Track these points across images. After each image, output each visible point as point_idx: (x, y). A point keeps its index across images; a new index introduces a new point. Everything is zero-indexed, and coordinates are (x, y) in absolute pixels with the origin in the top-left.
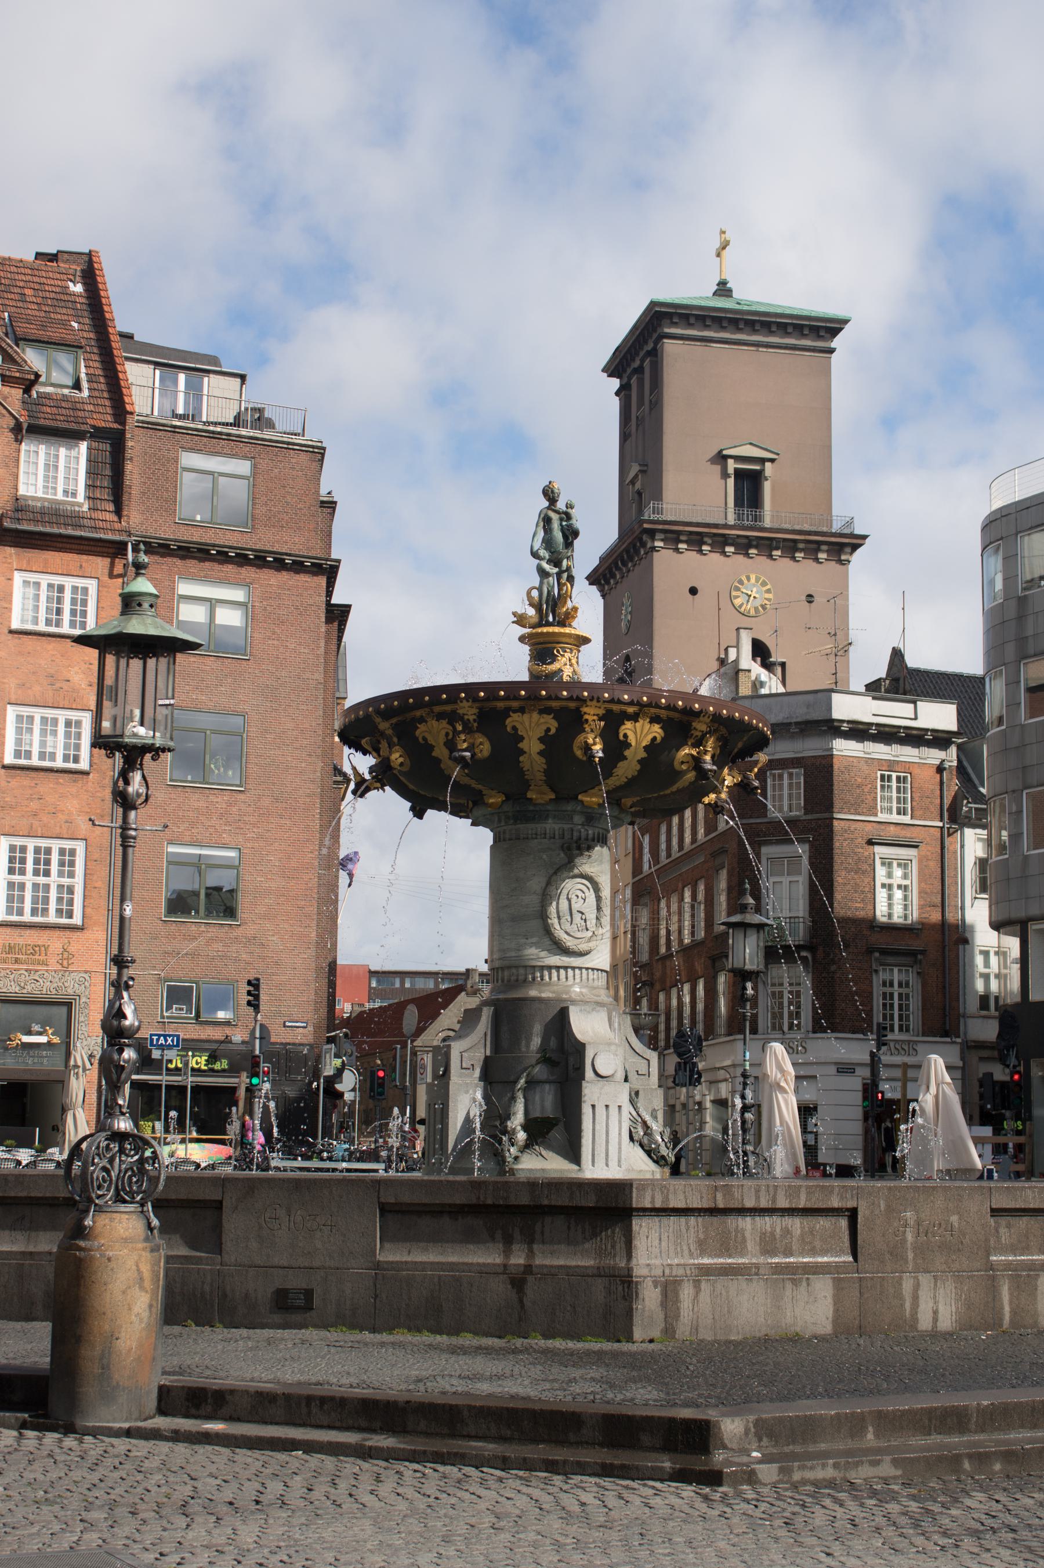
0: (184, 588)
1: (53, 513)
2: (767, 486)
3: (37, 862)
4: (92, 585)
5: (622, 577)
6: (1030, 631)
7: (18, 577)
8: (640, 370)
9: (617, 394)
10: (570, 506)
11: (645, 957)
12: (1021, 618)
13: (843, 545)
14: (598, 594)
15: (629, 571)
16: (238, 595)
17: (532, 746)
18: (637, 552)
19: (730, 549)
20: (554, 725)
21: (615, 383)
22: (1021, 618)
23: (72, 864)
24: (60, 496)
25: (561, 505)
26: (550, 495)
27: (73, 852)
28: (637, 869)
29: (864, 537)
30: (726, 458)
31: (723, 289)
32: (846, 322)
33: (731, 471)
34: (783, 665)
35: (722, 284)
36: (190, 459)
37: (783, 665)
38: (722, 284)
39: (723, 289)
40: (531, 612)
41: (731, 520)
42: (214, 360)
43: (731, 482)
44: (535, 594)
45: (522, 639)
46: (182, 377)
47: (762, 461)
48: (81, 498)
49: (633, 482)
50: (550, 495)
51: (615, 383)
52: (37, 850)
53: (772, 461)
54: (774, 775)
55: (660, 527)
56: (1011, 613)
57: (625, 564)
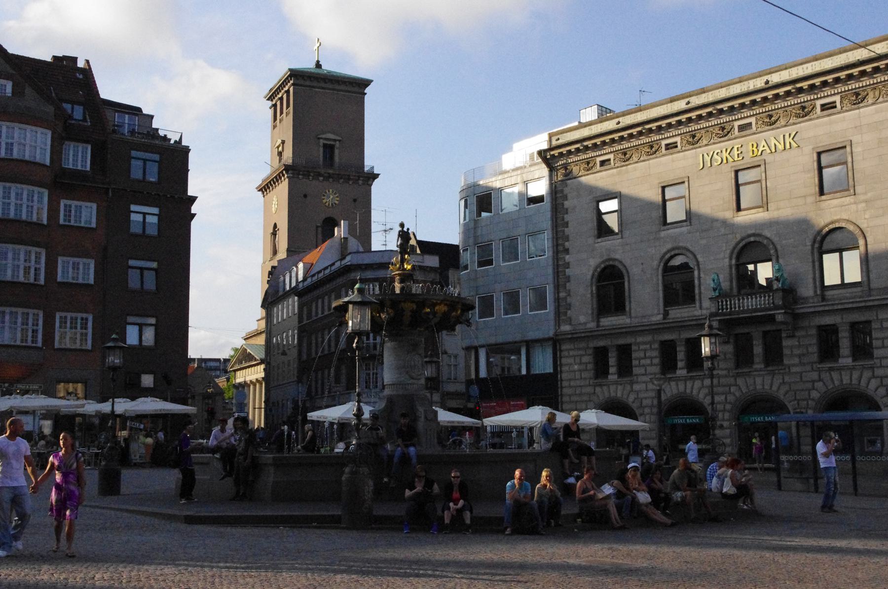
0: (133, 208)
1: (76, 174)
2: (337, 152)
3: (71, 323)
4: (94, 206)
6: (479, 233)
7: (63, 203)
8: (281, 99)
11: (305, 357)
12: (475, 228)
16: (156, 210)
17: (408, 314)
18: (280, 178)
19: (321, 178)
20: (415, 307)
21: (270, 103)
22: (475, 228)
23: (86, 324)
24: (79, 168)
25: (405, 229)
26: (402, 225)
27: (87, 319)
28: (300, 321)
29: (378, 175)
31: (318, 65)
32: (372, 81)
33: (321, 144)
35: (318, 62)
36: (134, 153)
38: (318, 62)
39: (318, 65)
42: (139, 110)
43: (321, 149)
46: (127, 116)
47: (335, 140)
48: (88, 169)
50: (402, 225)
51: (270, 103)
52: (72, 318)
53: (340, 141)
56: (472, 225)
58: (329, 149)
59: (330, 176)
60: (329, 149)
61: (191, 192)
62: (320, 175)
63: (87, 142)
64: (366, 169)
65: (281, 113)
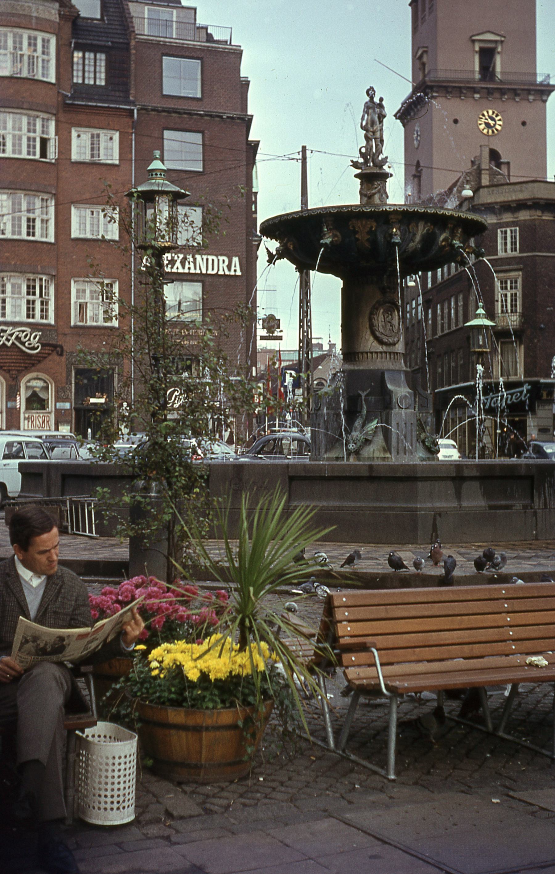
5: (414, 115)
9: (410, 5)
10: (381, 99)
13: (544, 91)
14: (401, 124)
15: (418, 110)
19: (477, 96)
26: (370, 92)
30: (474, 41)
33: (477, 49)
34: (508, 163)
37: (508, 163)
40: (361, 160)
41: (477, 76)
44: (363, 150)
45: (356, 176)
47: (496, 42)
49: (421, 57)
50: (370, 92)
53: (502, 42)
54: (502, 232)
55: (436, 84)
57: (416, 107)
58: (487, 55)
59: (490, 92)
60: (487, 55)
61: (249, 113)
62: (474, 90)
63: (95, 49)
64: (539, 79)
65: (424, 10)
